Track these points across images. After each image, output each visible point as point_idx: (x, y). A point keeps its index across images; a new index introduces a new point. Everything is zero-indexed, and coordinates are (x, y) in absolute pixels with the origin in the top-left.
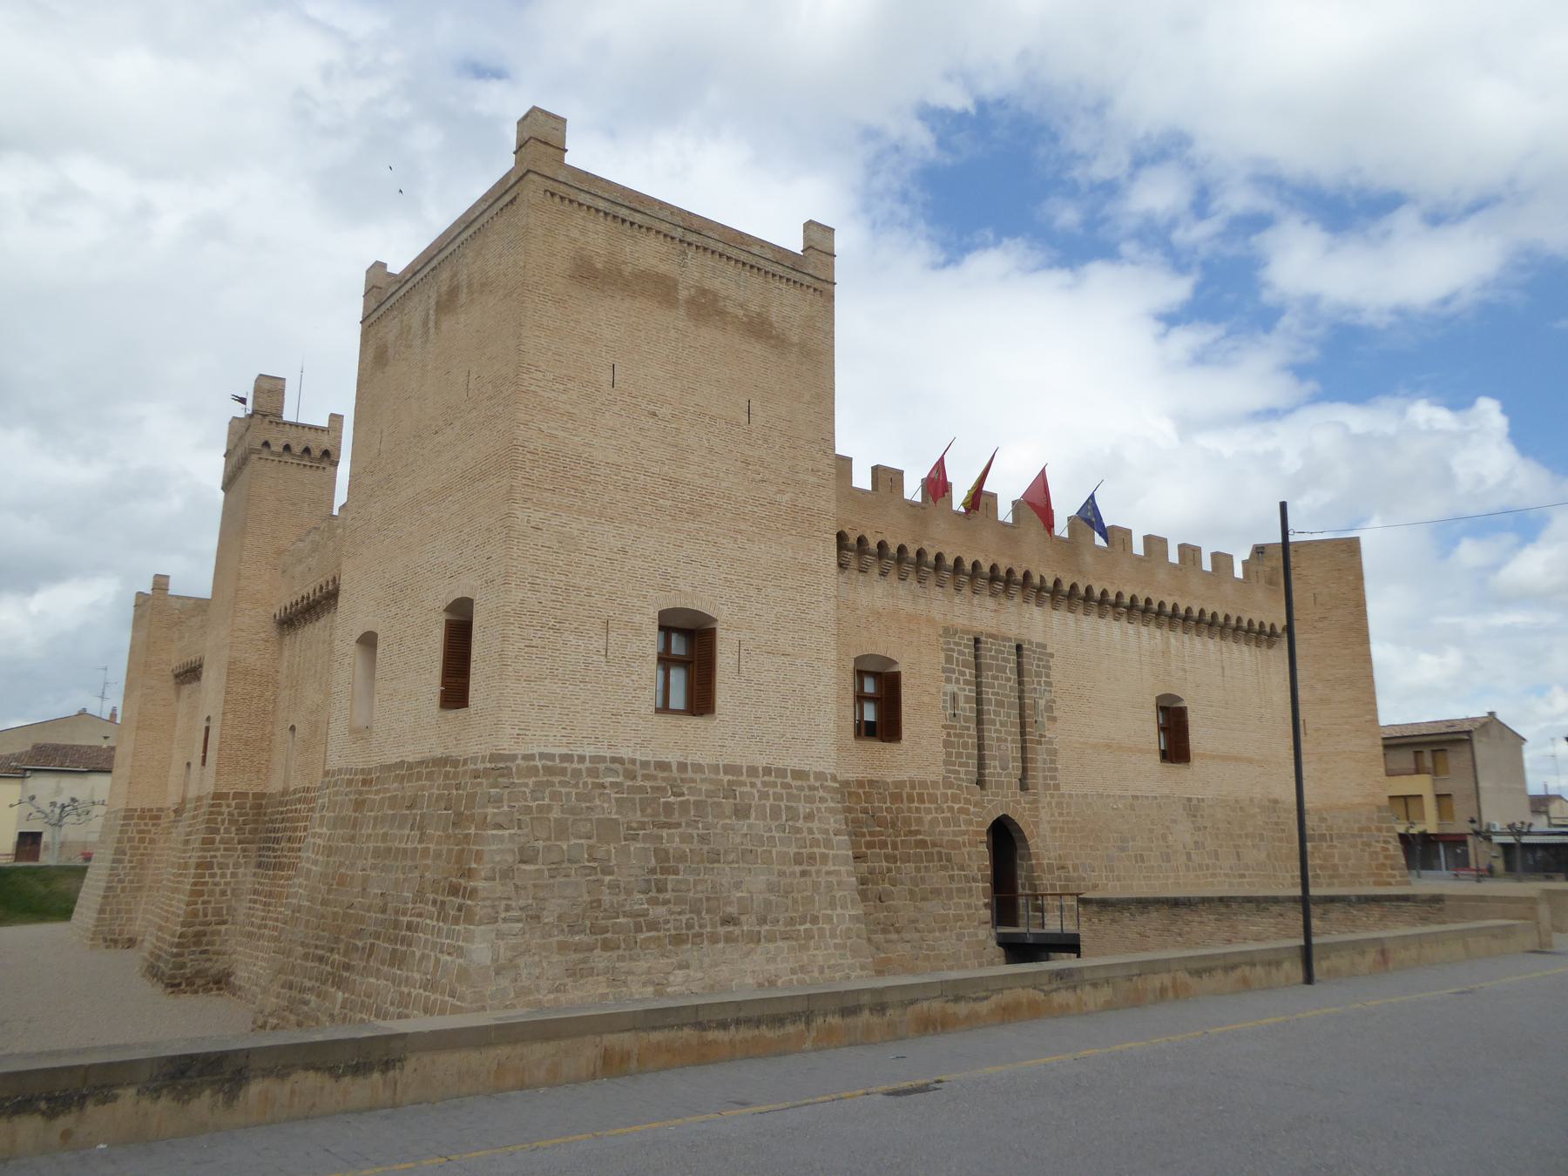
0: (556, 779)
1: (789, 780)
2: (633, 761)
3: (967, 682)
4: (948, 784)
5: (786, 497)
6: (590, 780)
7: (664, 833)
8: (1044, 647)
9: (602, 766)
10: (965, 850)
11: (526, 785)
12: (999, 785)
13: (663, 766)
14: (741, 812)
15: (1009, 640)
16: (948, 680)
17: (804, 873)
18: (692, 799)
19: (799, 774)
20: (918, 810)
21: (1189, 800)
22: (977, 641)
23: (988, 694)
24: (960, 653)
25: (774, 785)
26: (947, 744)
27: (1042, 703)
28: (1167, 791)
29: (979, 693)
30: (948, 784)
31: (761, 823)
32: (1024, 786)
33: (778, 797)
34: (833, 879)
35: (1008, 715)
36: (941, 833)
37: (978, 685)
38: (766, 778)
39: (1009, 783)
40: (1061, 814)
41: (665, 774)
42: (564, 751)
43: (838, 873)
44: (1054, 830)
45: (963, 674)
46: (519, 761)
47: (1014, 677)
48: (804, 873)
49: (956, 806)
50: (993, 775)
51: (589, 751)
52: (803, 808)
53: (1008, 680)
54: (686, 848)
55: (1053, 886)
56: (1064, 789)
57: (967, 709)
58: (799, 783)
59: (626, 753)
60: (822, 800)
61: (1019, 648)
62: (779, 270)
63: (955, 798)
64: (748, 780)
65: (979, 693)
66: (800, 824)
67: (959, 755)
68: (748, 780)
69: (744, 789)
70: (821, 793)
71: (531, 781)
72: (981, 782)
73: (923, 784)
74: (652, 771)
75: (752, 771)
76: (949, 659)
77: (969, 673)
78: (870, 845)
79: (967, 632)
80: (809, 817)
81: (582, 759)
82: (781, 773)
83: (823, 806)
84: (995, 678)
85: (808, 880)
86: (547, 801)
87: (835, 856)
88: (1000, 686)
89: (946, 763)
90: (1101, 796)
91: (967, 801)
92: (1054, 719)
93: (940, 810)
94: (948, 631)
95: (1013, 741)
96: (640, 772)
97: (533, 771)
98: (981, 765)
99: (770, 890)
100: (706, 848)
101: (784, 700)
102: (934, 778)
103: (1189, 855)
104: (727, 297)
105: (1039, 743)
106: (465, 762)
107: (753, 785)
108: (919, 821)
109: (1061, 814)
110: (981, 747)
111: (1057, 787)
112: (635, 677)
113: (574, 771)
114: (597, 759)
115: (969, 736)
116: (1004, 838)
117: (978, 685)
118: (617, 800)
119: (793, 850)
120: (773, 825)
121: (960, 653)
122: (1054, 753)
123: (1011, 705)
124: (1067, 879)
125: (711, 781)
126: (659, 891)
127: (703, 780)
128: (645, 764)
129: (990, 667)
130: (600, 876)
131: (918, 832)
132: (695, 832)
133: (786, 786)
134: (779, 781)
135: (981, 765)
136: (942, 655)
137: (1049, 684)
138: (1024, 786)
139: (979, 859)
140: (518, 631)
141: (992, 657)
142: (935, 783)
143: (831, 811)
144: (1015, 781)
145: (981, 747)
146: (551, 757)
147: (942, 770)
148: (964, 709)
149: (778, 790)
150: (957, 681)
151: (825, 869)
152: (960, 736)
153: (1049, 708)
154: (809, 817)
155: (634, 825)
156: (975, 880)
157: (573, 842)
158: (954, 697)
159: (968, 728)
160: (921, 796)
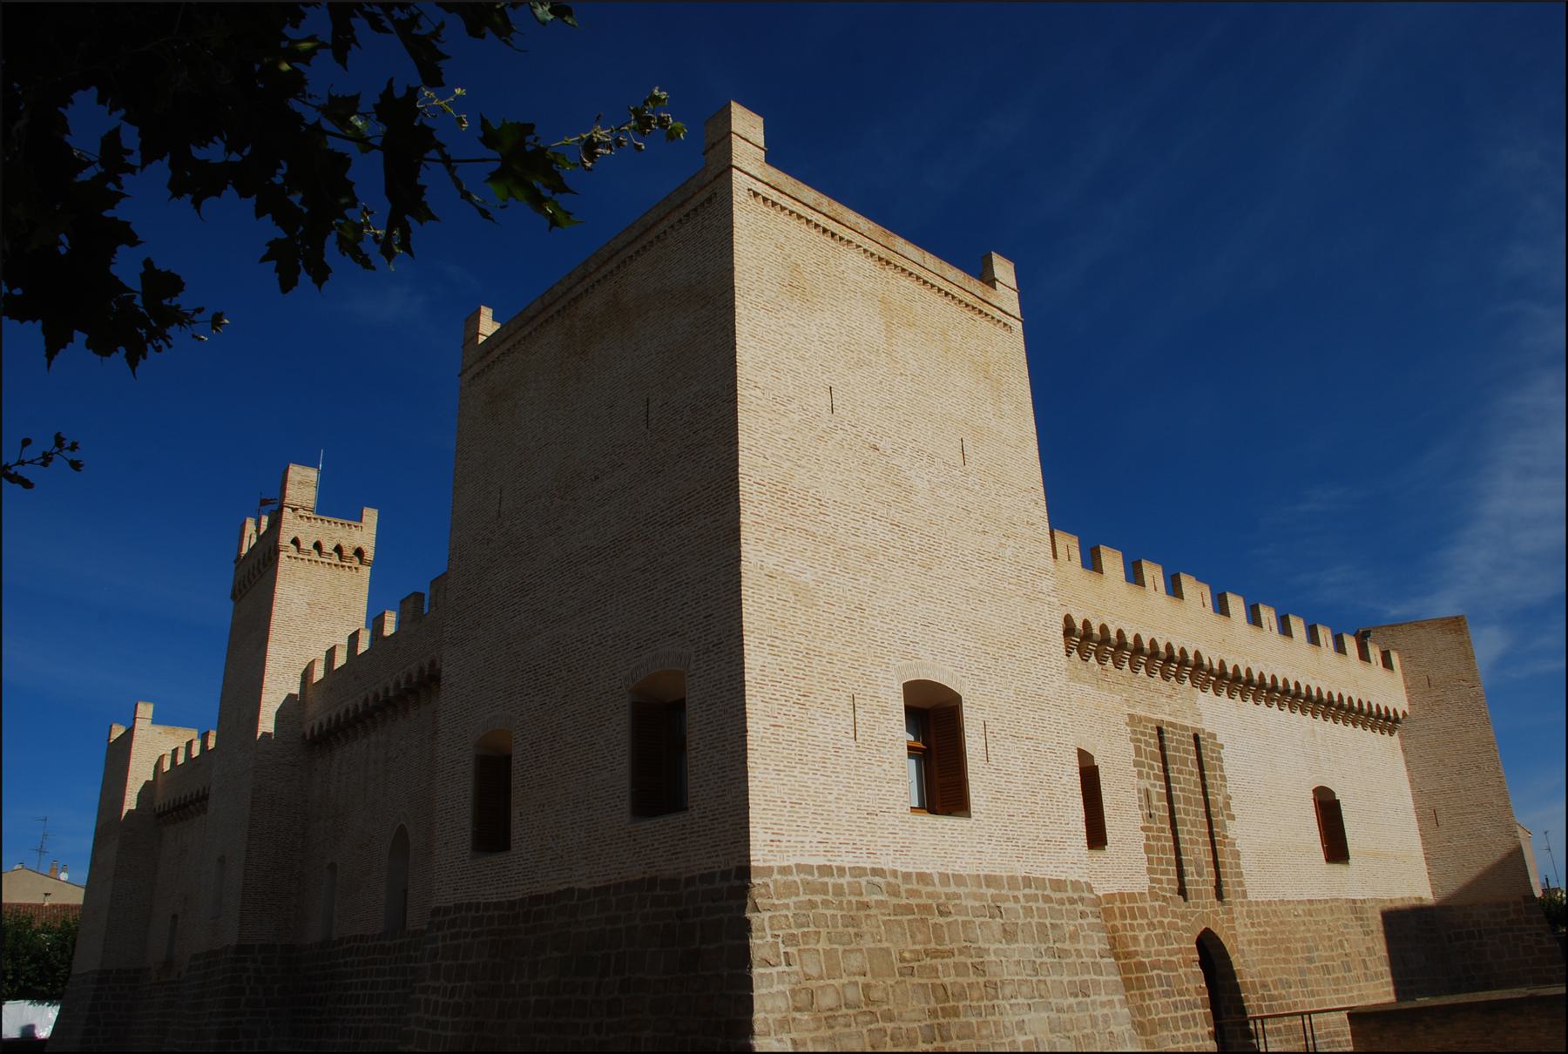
0: (818, 898)
2: (894, 873)
3: (1156, 777)
4: (1154, 896)
6: (854, 899)
7: (937, 962)
9: (863, 881)
10: (1181, 971)
11: (787, 906)
12: (1199, 894)
13: (923, 878)
14: (1009, 934)
15: (1185, 728)
18: (960, 919)
19: (1058, 885)
21: (1354, 901)
22: (1160, 731)
24: (1148, 744)
25: (1035, 898)
26: (1148, 849)
27: (1220, 798)
29: (1169, 789)
30: (1154, 896)
31: (1030, 946)
32: (1219, 895)
37: (1167, 779)
38: (1027, 891)
40: (1253, 925)
41: (930, 889)
42: (822, 861)
43: (1111, 1002)
44: (1250, 943)
45: (1151, 767)
46: (776, 876)
47: (1196, 770)
49: (1166, 921)
51: (847, 861)
52: (1068, 926)
53: (1191, 773)
54: (964, 980)
55: (1260, 1007)
56: (1251, 897)
58: (1058, 895)
59: (886, 863)
60: (1083, 915)
61: (1196, 737)
64: (1010, 893)
65: (1169, 789)
66: (1067, 945)
68: (1010, 893)
69: (1007, 905)
70: (1080, 907)
71: (791, 901)
72: (1182, 891)
73: (1132, 896)
74: (915, 886)
76: (1138, 750)
77: (1158, 765)
79: (1150, 720)
80: (1074, 937)
81: (841, 870)
82: (1040, 883)
84: (1180, 772)
86: (812, 929)
87: (1106, 982)
88: (1185, 782)
89: (1150, 871)
92: (1232, 817)
93: (1151, 925)
94: (1133, 720)
95: (1204, 844)
96: (903, 888)
97: (790, 889)
98: (1181, 873)
99: (1052, 1031)
100: (981, 980)
101: (1034, 794)
106: (690, 881)
107: (1016, 899)
110: (1178, 852)
112: (886, 766)
113: (834, 885)
114: (858, 872)
115: (1166, 839)
116: (1212, 955)
117: (1167, 779)
118: (885, 923)
119: (1066, 978)
120: (1043, 947)
121: (1148, 744)
122: (1237, 855)
124: (1272, 998)
125: (975, 897)
126: (943, 1040)
127: (967, 896)
128: (907, 877)
130: (881, 1024)
132: (969, 961)
133: (1048, 899)
134: (1040, 892)
135: (1181, 873)
137: (1223, 778)
138: (1219, 895)
139: (1192, 979)
140: (761, 705)
142: (1141, 894)
143: (1092, 927)
144: (1211, 888)
145: (1178, 852)
146: (808, 869)
148: (1157, 809)
152: (1158, 839)
154: (1074, 937)
155: (907, 955)
157: (845, 980)
159: (1163, 830)
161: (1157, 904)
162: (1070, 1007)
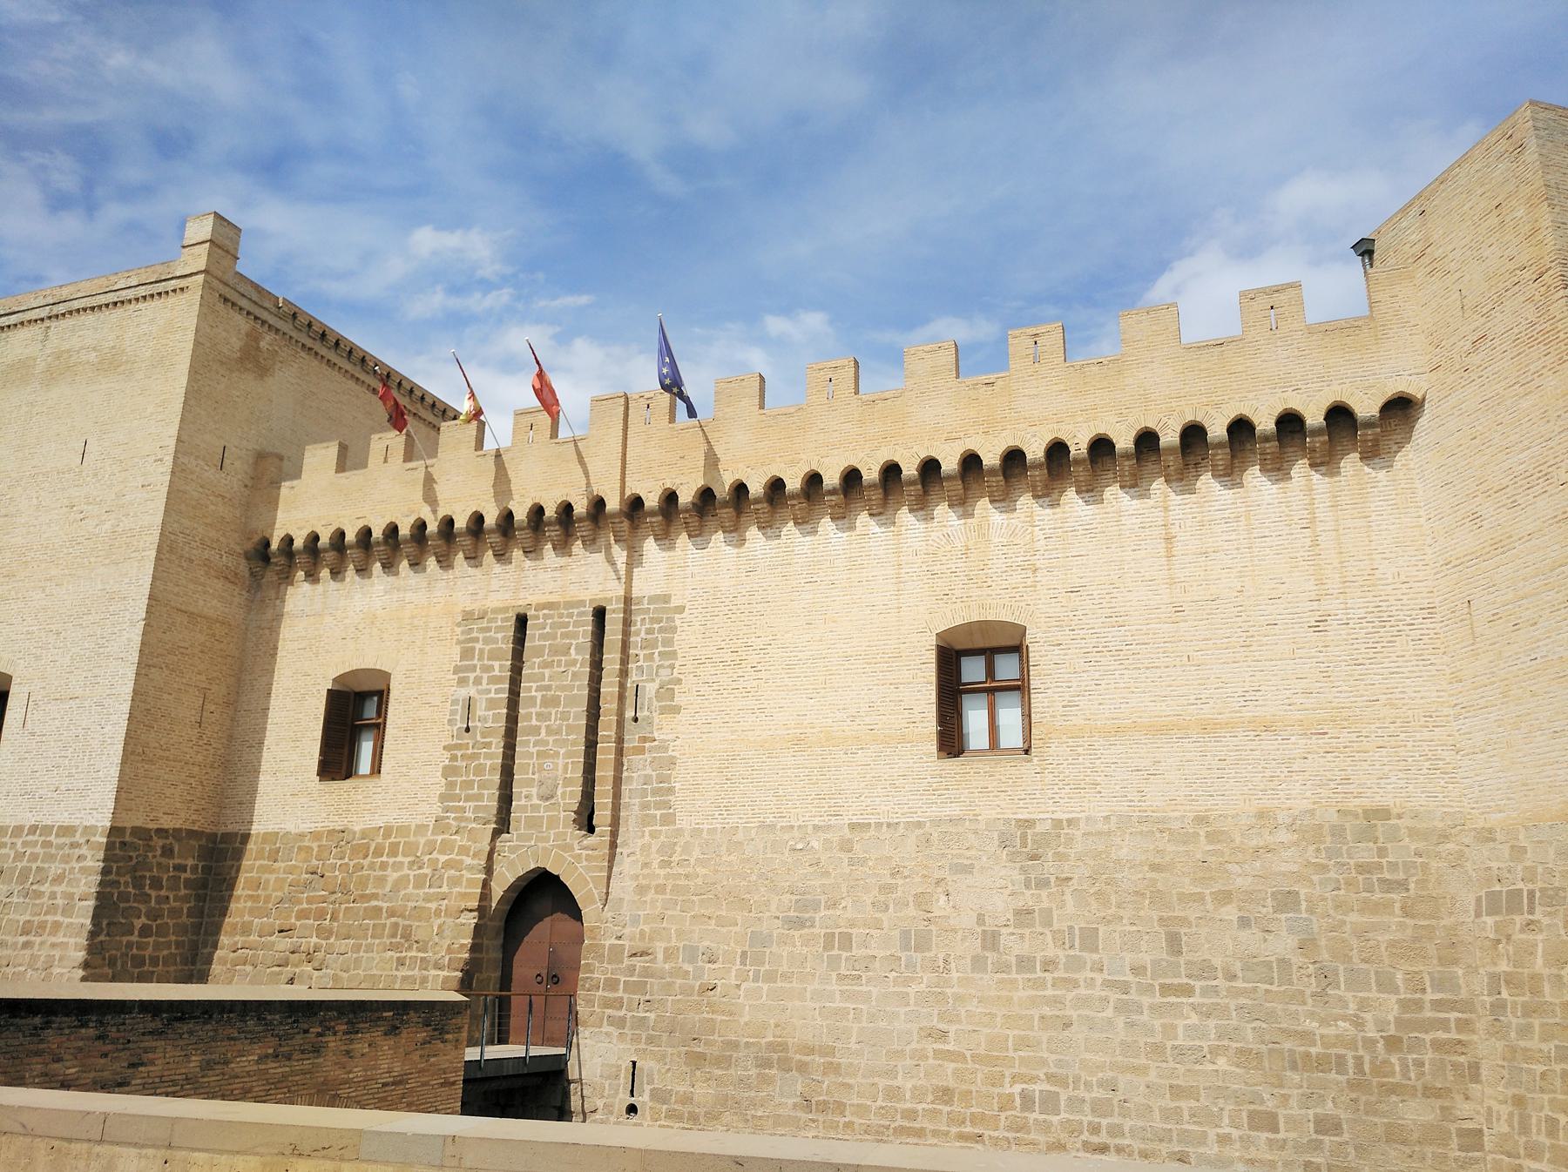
1: (52, 838)
5: (107, 526)
8: (666, 598)
12: (534, 823)
15: (582, 603)
16: (462, 682)
17: (26, 945)
19: (66, 830)
20: (384, 866)
21: (1029, 823)
23: (529, 689)
27: (650, 689)
28: (955, 810)
33: (34, 857)
34: (57, 953)
35: (564, 716)
36: (407, 898)
38: (30, 838)
39: (553, 822)
40: (665, 864)
44: (642, 890)
48: (26, 945)
49: (443, 858)
50: (524, 809)
52: (55, 869)
56: (684, 822)
57: (491, 718)
58: (63, 840)
62: (142, 291)
63: (446, 847)
67: (469, 784)
70: (84, 851)
73: (403, 830)
75: (18, 830)
76: (467, 654)
78: (303, 915)
80: (58, 880)
82: (47, 830)
83: (77, 866)
85: (27, 952)
90: (772, 827)
91: (464, 850)
95: (569, 755)
102: (419, 820)
103: (991, 940)
104: (82, 348)
105: (641, 751)
108: (382, 880)
109: (665, 864)
111: (668, 820)
123: (571, 701)
129: (539, 652)
131: (374, 896)
135: (506, 799)
136: (457, 650)
141: (543, 637)
142: (421, 828)
147: (437, 809)
149: (38, 850)
150: (478, 681)
151: (53, 939)
153: (666, 692)
154: (58, 880)
156: (438, 967)
158: (469, 705)
159: (488, 745)
160: (394, 846)
161: (440, 838)
162: (16, 944)
